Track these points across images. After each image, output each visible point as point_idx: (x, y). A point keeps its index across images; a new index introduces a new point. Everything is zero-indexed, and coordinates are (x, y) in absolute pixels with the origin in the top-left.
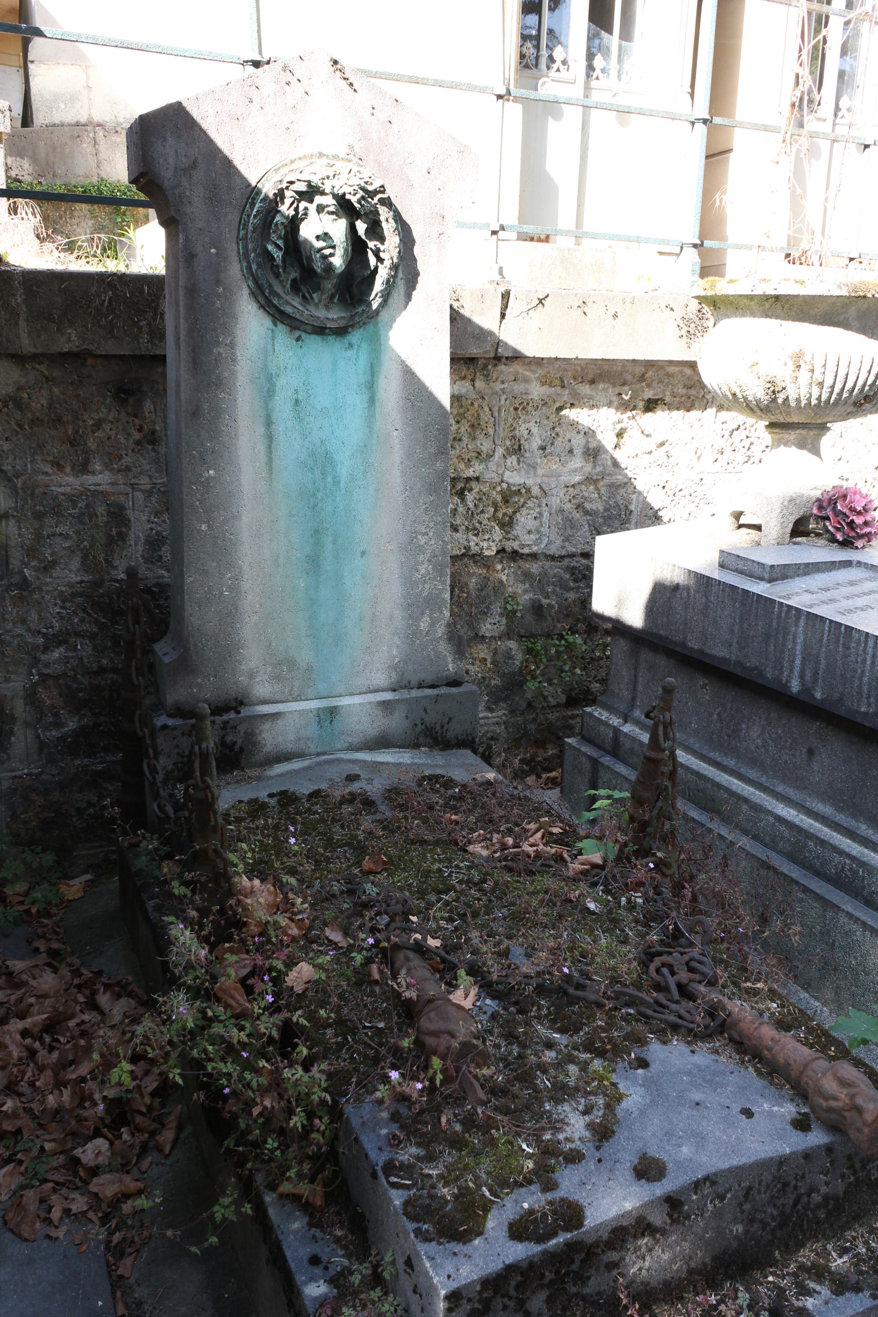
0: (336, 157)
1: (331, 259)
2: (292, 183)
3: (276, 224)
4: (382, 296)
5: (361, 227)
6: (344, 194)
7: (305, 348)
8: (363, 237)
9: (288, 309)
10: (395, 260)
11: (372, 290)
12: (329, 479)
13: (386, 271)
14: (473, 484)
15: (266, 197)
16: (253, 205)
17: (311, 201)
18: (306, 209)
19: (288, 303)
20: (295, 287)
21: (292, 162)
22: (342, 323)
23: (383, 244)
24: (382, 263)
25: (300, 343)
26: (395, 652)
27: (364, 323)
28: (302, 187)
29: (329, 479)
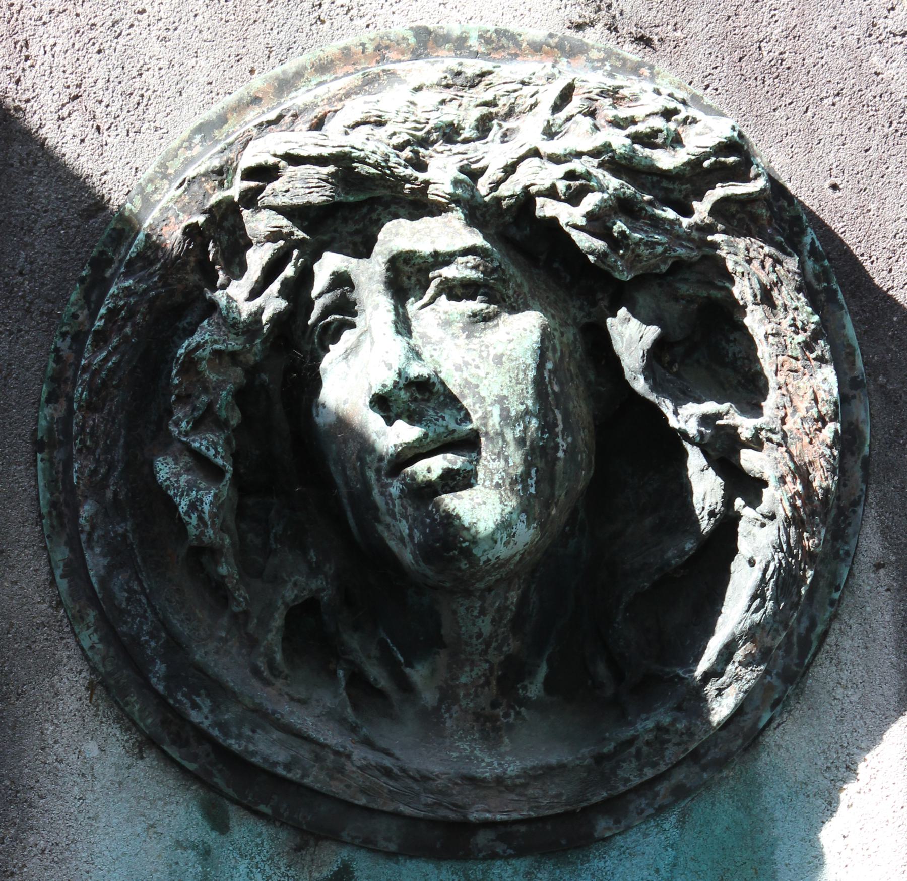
0: (501, 43)
1: (458, 503)
2: (264, 174)
3: (190, 364)
4: (763, 656)
5: (631, 336)
6: (527, 199)
8: (640, 385)
9: (266, 748)
10: (820, 480)
11: (709, 631)
13: (771, 533)
15: (153, 247)
16: (95, 287)
17: (362, 248)
18: (341, 280)
19: (264, 718)
20: (311, 639)
21: (284, 85)
22: (551, 798)
23: (755, 410)
24: (754, 500)
27: (681, 793)
28: (302, 186)
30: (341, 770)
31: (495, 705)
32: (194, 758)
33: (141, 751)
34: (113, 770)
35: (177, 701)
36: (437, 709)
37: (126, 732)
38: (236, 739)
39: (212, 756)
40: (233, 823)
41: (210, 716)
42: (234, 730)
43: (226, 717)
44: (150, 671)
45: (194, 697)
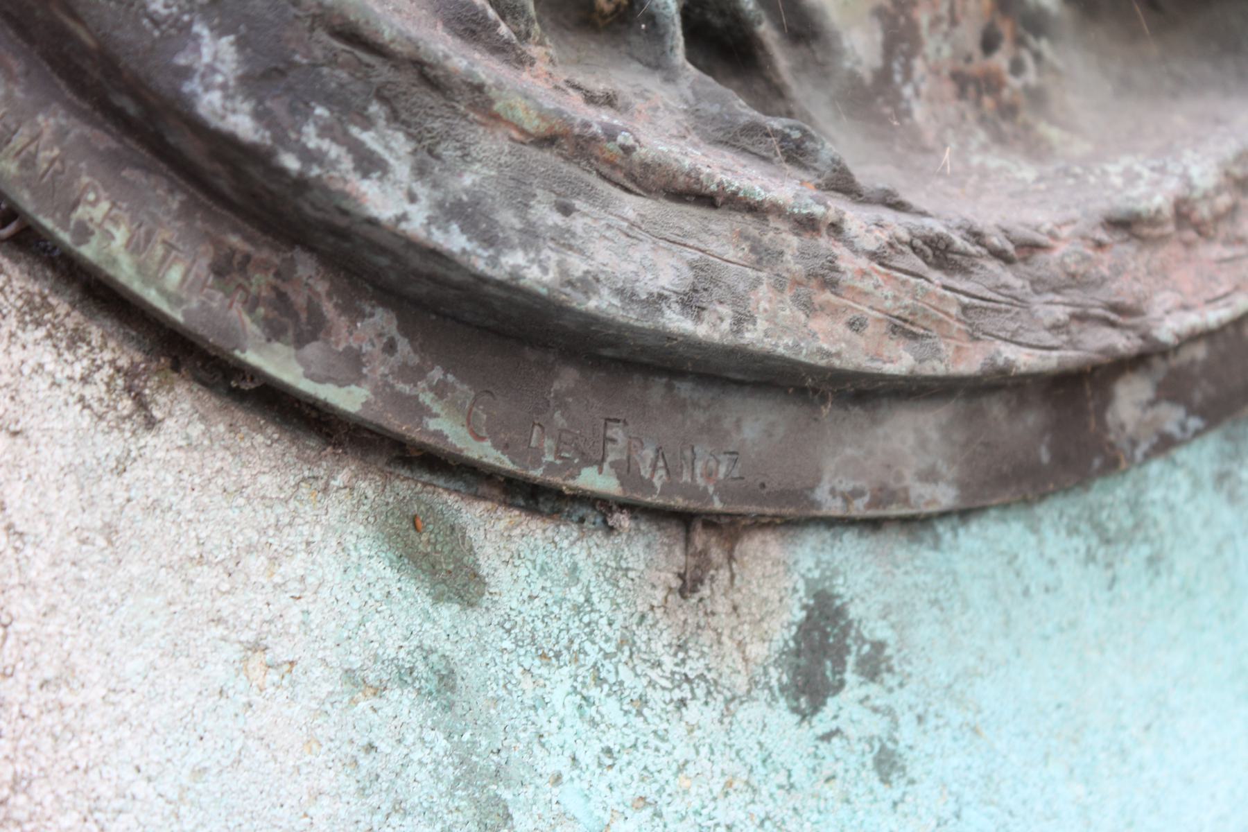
7: (935, 756)
25: (849, 704)
30: (828, 278)
31: (989, 43)
32: (352, 366)
33: (141, 404)
34: (70, 492)
35: (309, 156)
36: (884, 76)
37: (72, 344)
38: (525, 246)
39: (403, 345)
40: (488, 559)
41: (421, 190)
42: (508, 218)
43: (468, 180)
44: (186, 73)
45: (355, 131)
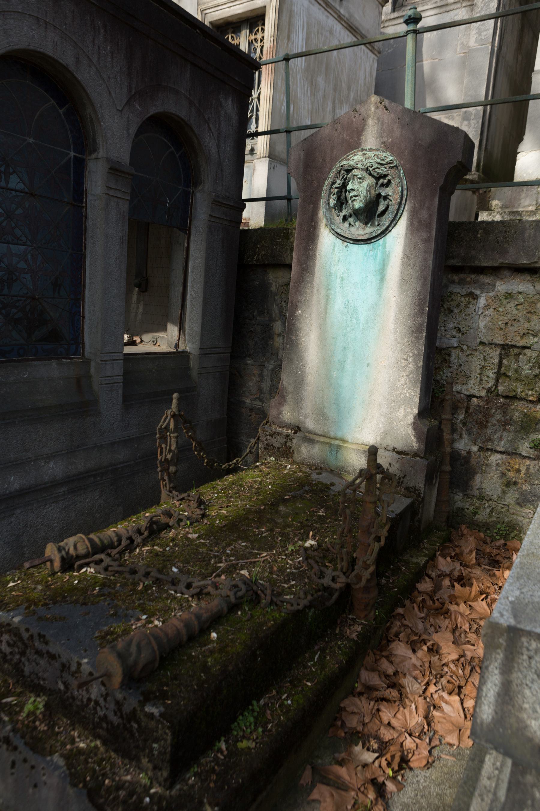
12: (355, 321)
14: (527, 351)
22: (366, 237)
26: (381, 426)
29: (355, 321)
